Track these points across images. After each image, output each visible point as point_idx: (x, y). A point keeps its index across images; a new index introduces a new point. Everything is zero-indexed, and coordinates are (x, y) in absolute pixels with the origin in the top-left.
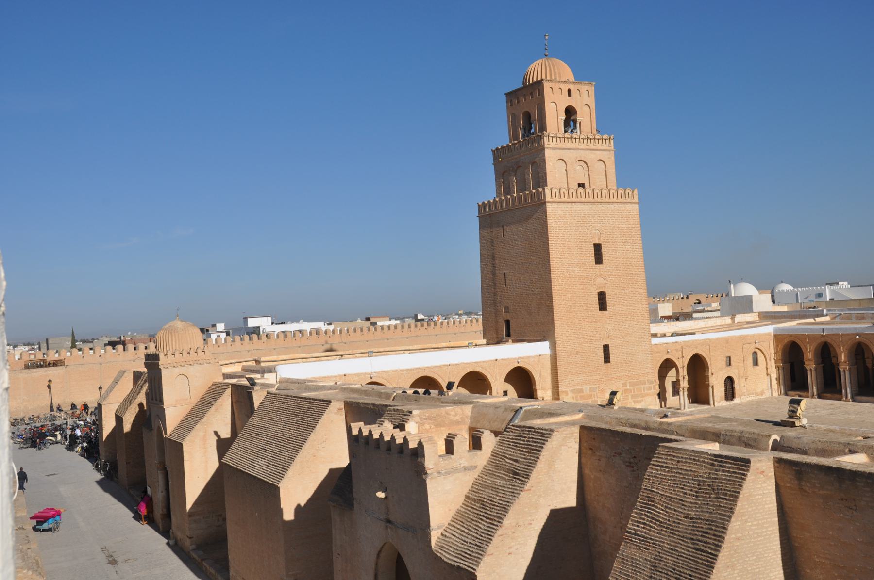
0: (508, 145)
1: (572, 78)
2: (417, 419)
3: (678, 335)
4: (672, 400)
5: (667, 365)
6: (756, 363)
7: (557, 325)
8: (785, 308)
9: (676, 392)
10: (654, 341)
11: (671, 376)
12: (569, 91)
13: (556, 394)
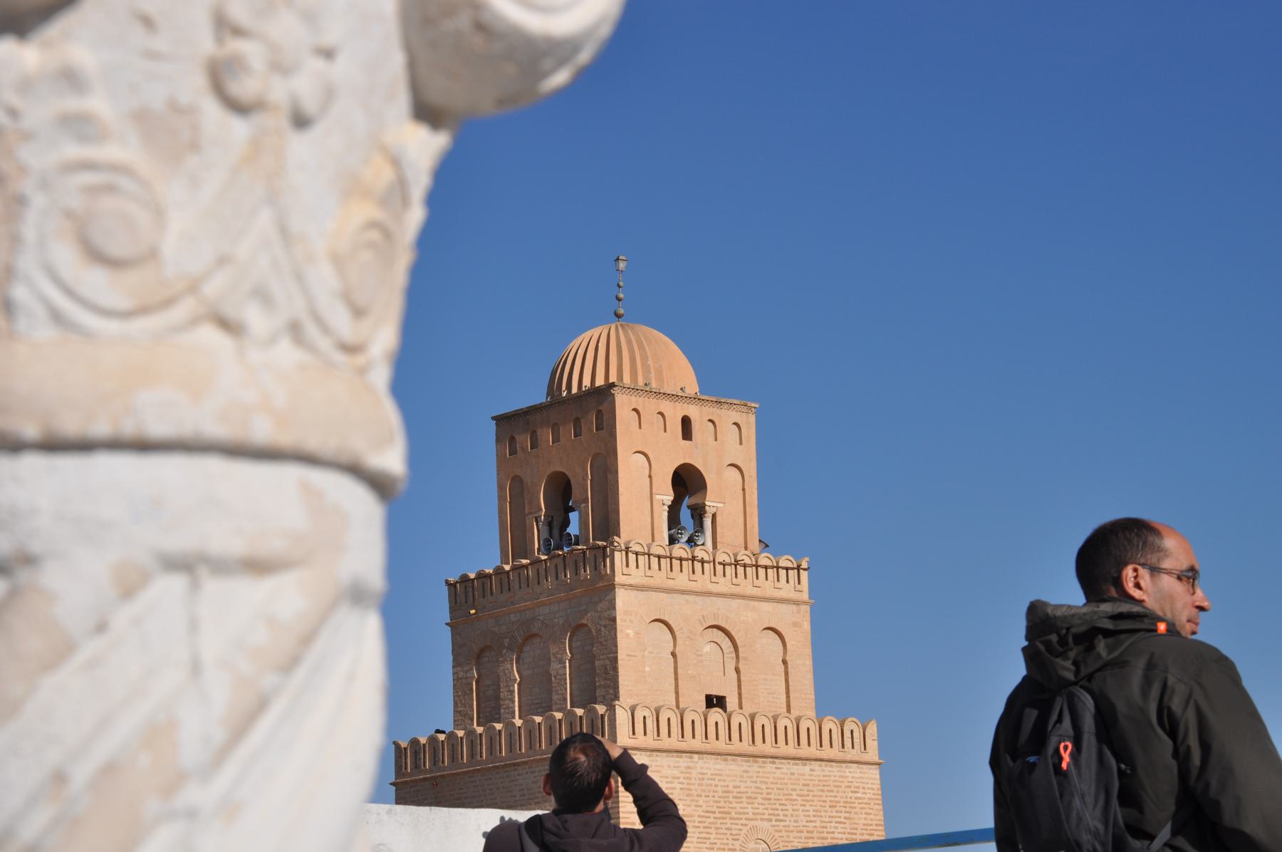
0: (499, 571)
1: (692, 388)
12: (686, 422)
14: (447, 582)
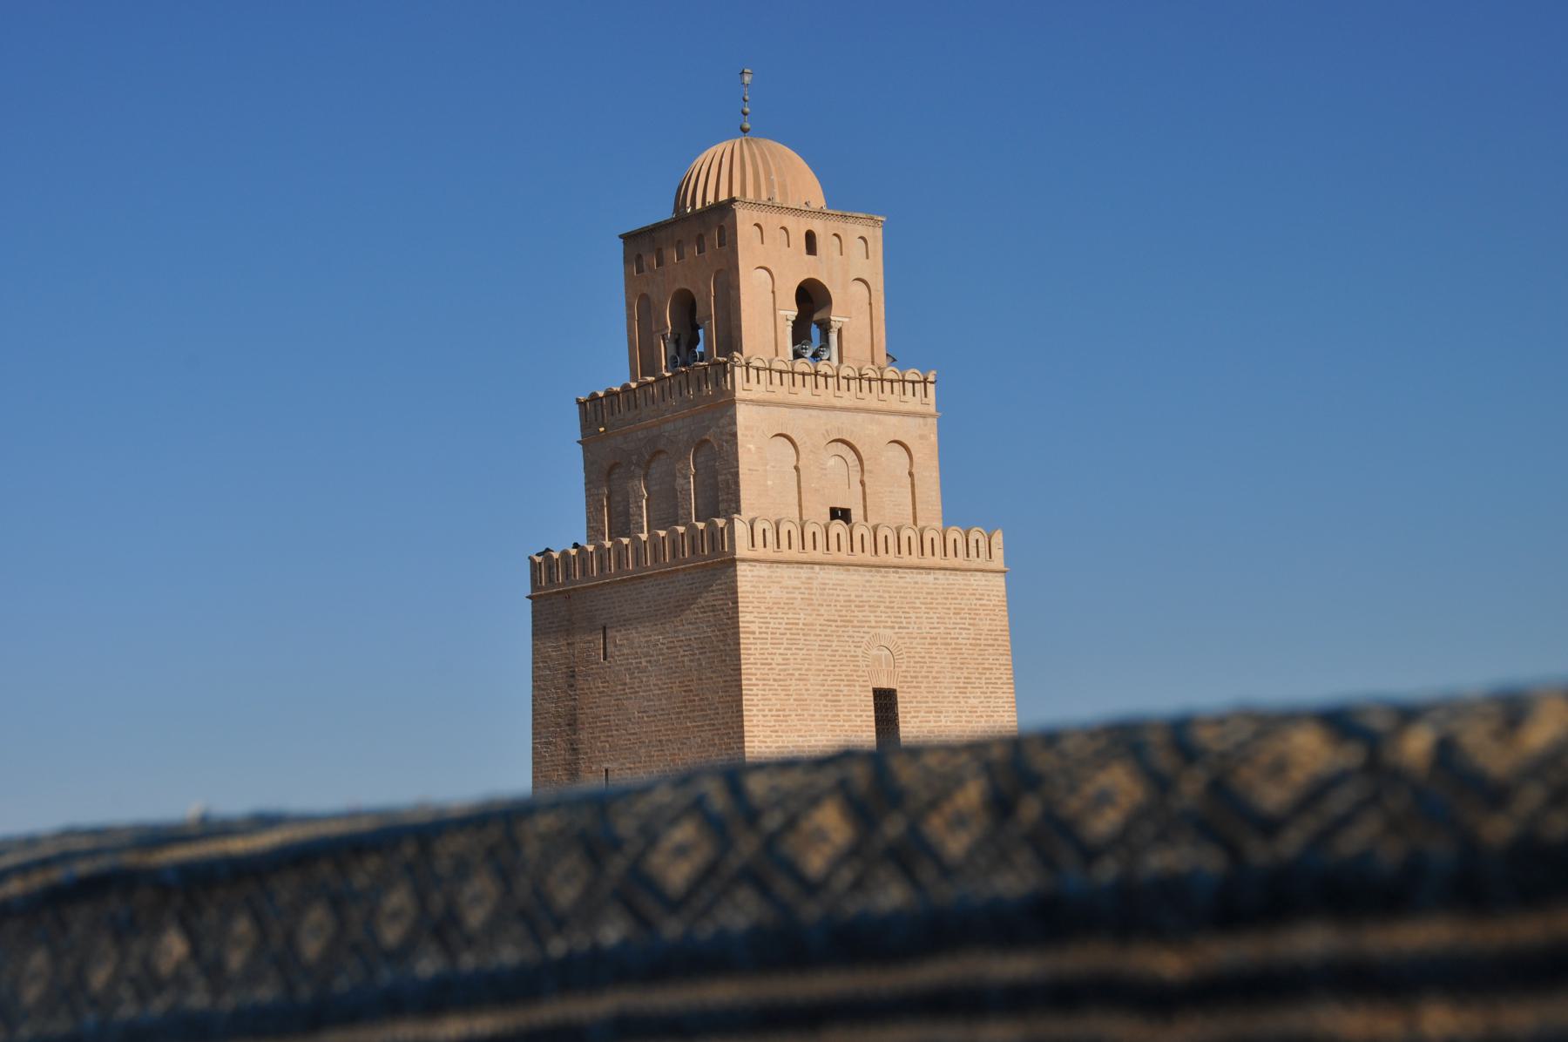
0: (626, 388)
1: (818, 202)
12: (810, 238)
14: (578, 401)
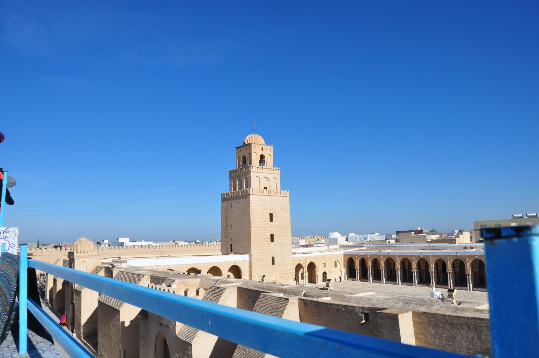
1: (264, 143)
2: (177, 283)
3: (304, 253)
4: (301, 281)
5: (299, 267)
6: (336, 266)
7: (252, 247)
8: (351, 243)
9: (302, 278)
10: (294, 256)
11: (301, 272)
13: (251, 277)
